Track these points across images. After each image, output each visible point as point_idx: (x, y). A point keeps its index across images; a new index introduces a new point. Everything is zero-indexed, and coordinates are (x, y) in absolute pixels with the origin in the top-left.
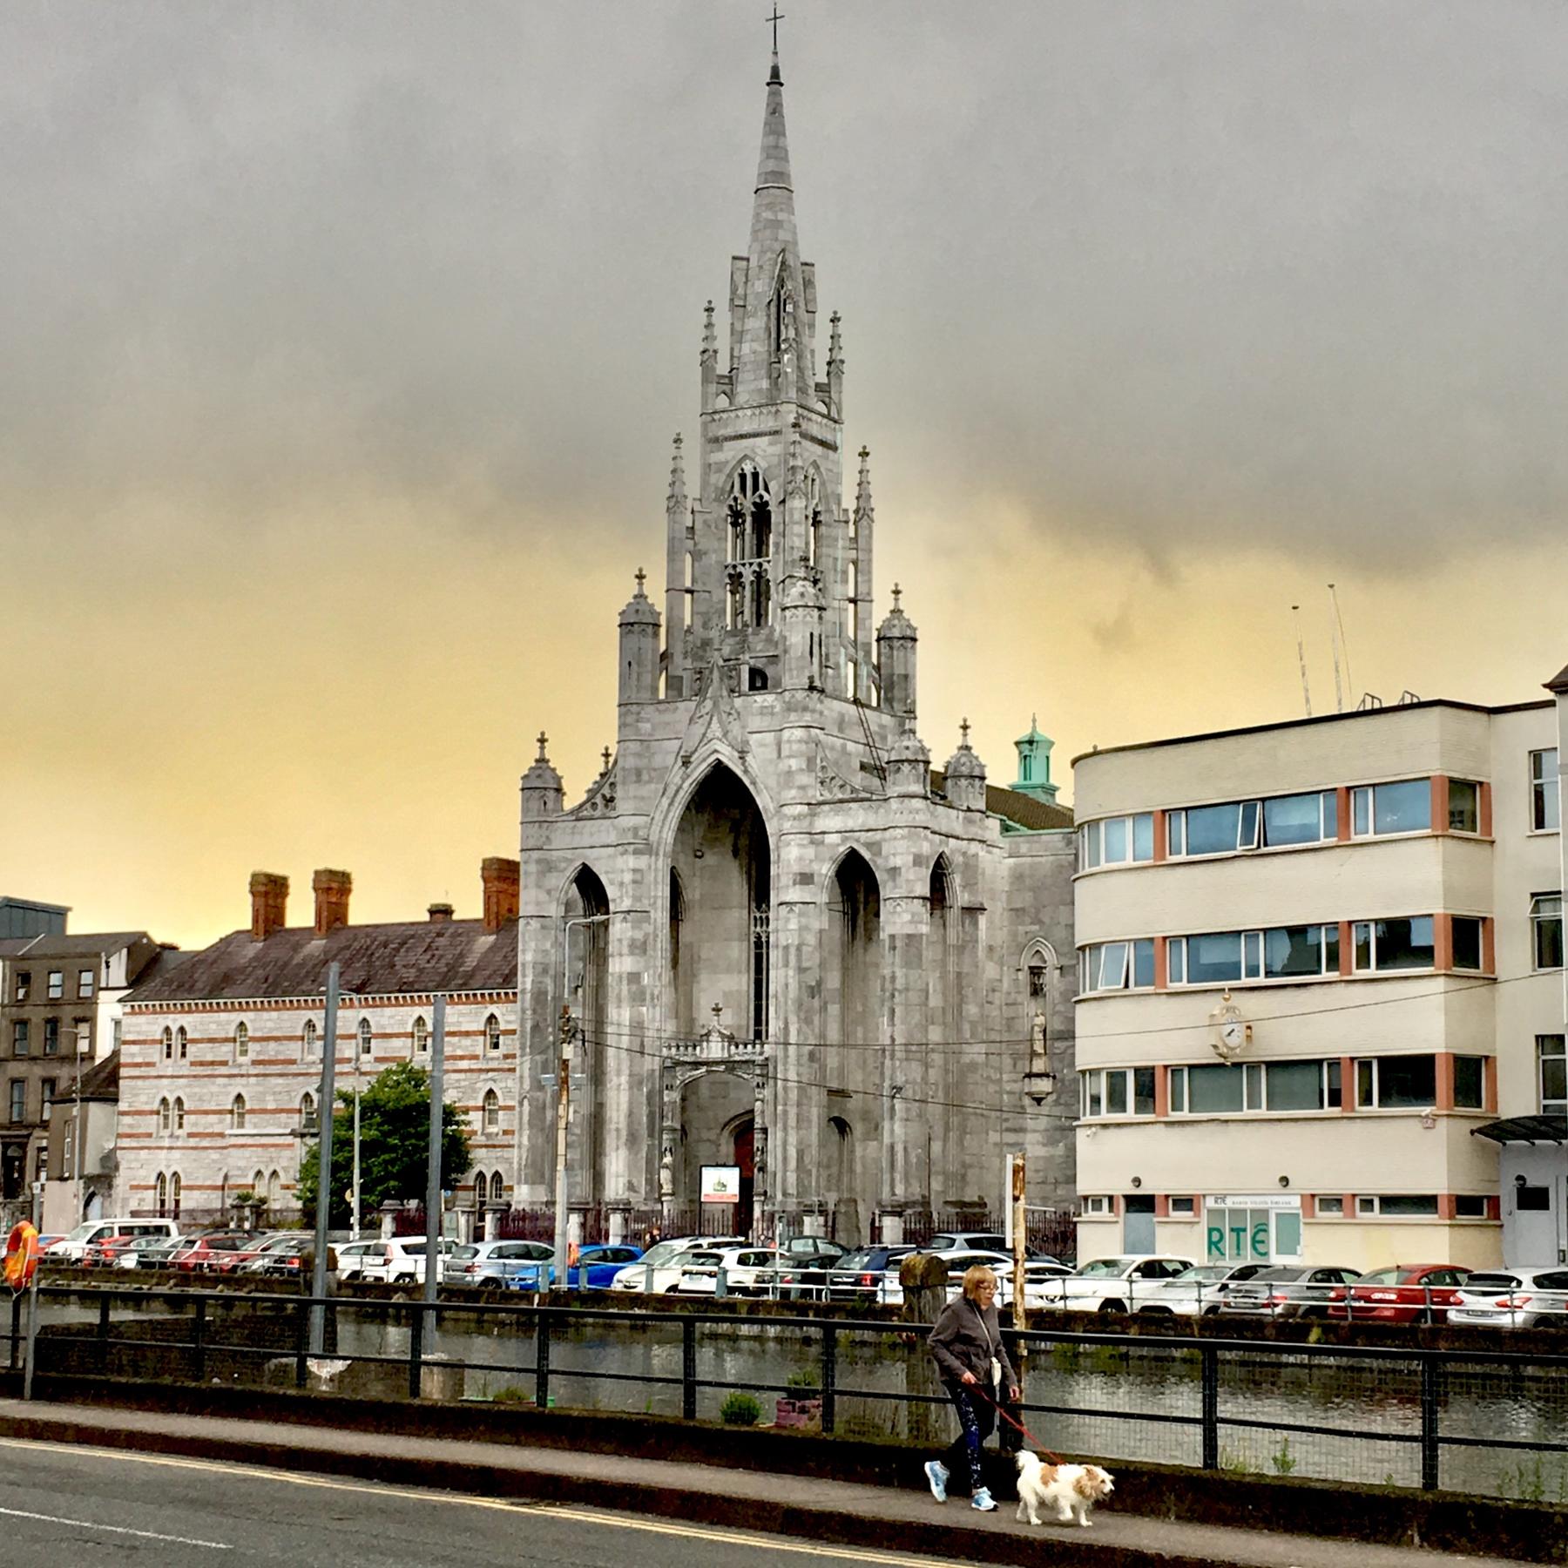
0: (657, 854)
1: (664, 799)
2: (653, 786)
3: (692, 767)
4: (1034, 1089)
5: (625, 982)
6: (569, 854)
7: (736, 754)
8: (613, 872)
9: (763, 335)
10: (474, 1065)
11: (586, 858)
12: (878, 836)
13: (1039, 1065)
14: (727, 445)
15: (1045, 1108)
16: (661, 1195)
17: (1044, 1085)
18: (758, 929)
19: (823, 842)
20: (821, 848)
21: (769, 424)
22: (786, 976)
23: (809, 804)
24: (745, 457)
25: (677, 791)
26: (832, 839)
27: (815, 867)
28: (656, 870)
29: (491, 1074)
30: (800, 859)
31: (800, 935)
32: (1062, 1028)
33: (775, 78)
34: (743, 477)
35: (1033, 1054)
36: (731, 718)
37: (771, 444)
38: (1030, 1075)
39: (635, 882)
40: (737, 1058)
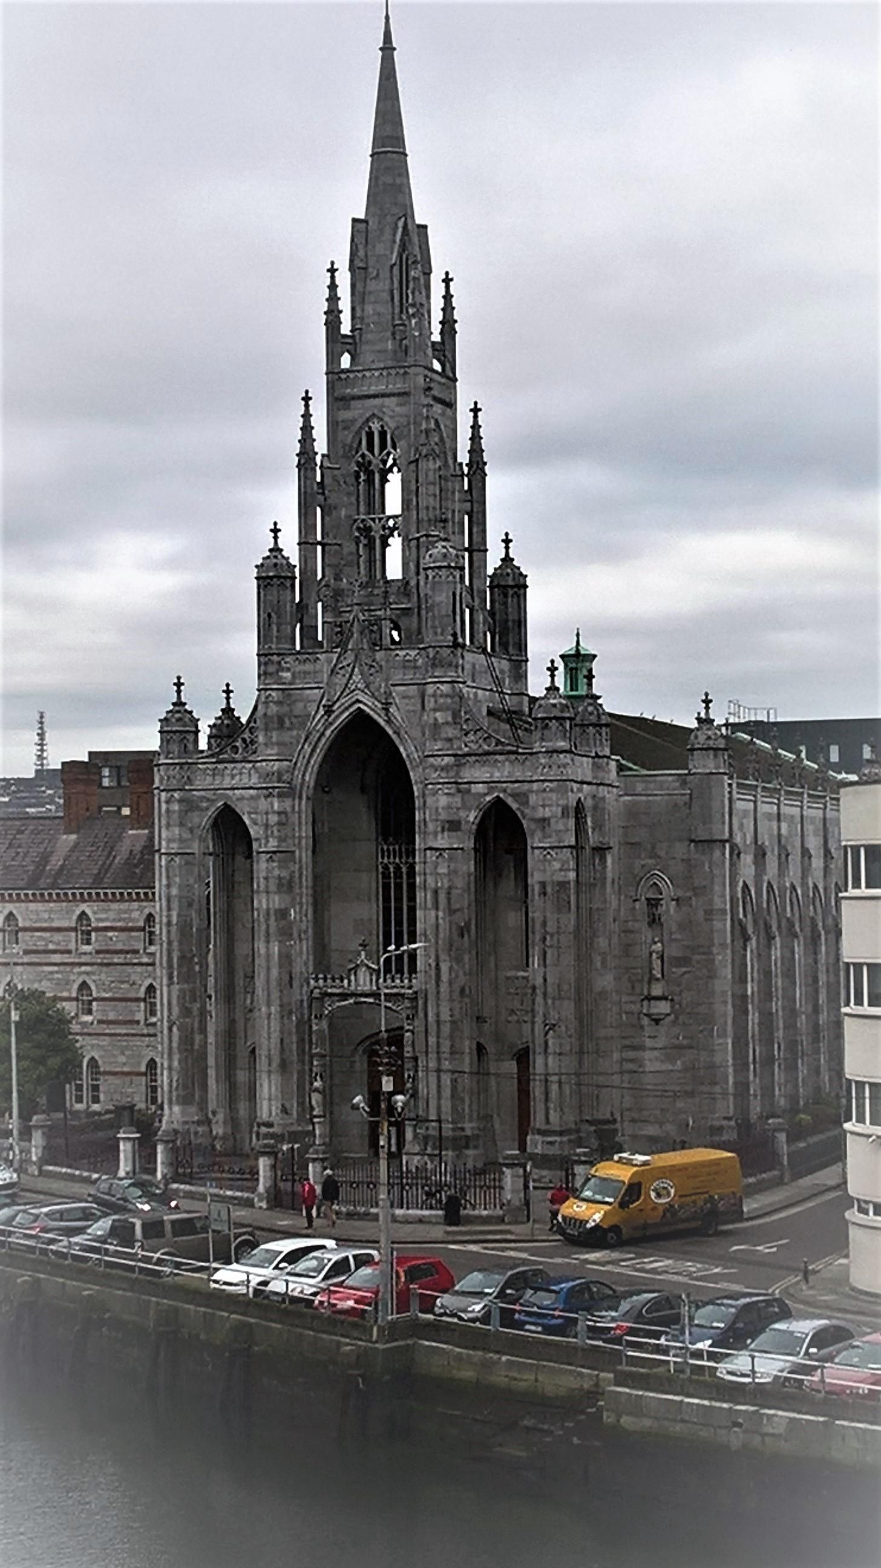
0: (300, 798)
2: (295, 733)
3: (333, 716)
4: (654, 1011)
5: (273, 918)
8: (256, 813)
9: (386, 296)
10: (66, 958)
11: (228, 797)
12: (526, 786)
13: (657, 990)
15: (662, 1029)
17: (663, 1007)
18: (386, 860)
20: (466, 797)
21: (399, 386)
22: (437, 917)
25: (319, 739)
26: (480, 788)
27: (462, 814)
28: (299, 812)
29: (83, 968)
30: (449, 807)
31: (450, 880)
32: (680, 955)
35: (652, 979)
36: (373, 670)
37: (401, 405)
38: (650, 998)
39: (280, 824)
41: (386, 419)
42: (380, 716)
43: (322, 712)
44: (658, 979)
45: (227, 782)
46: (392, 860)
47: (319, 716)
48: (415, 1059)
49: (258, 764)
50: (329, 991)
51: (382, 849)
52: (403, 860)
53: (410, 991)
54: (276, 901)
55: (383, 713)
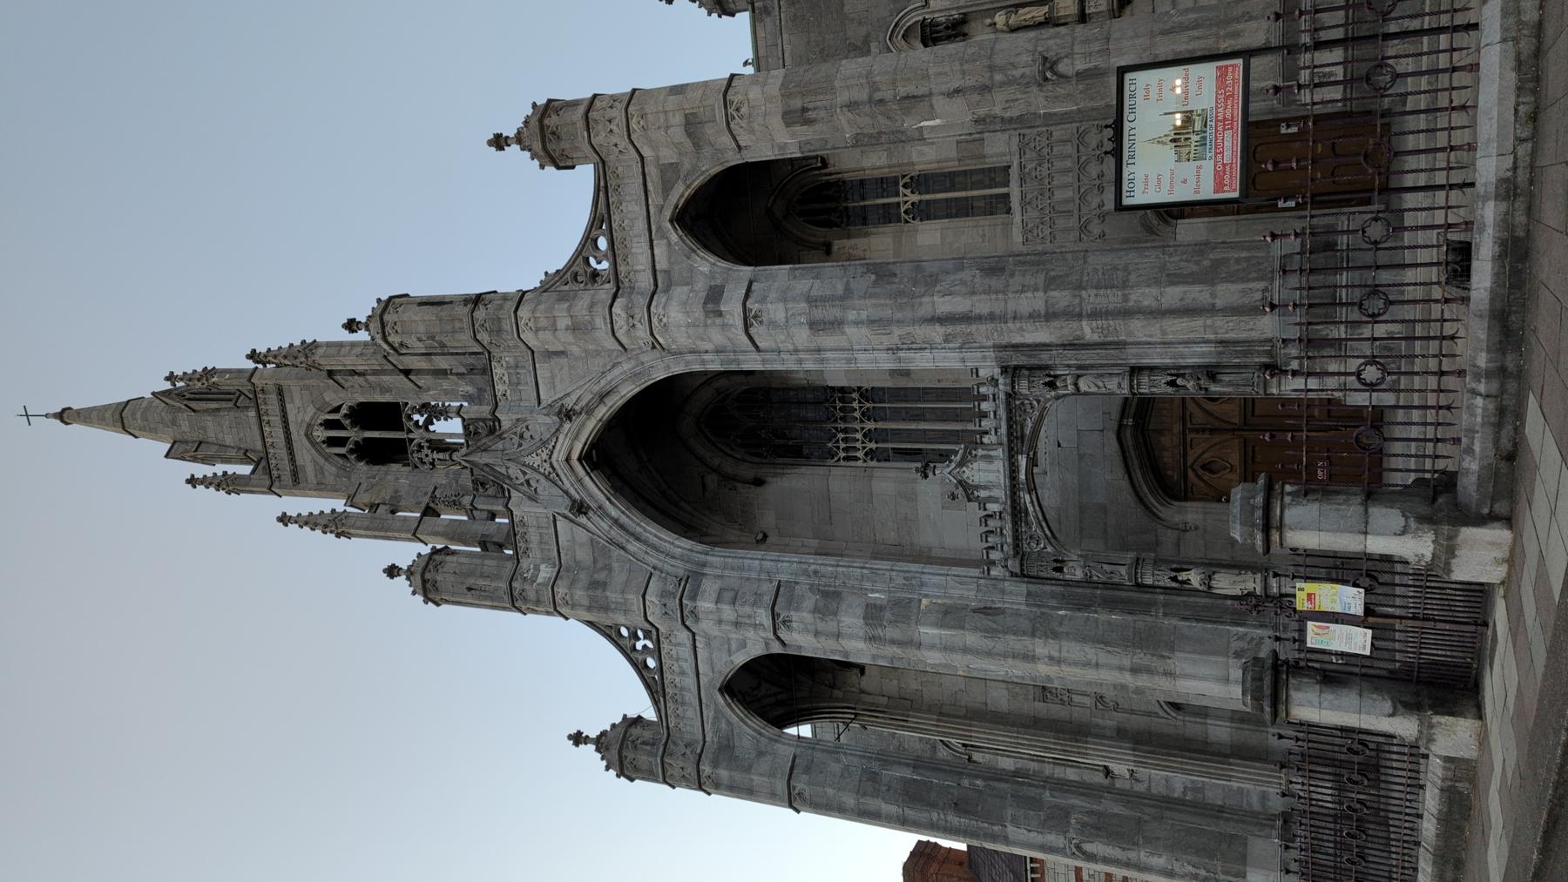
0: (704, 565)
1: (630, 547)
2: (615, 565)
5: (880, 632)
6: (709, 714)
7: (567, 426)
12: (652, 170)
14: (299, 461)
16: (1267, 596)
19: (665, 271)
23: (615, 297)
24: (308, 436)
25: (622, 527)
27: (701, 286)
31: (794, 299)
33: (64, 416)
34: (332, 442)
36: (527, 435)
40: (1003, 430)
41: (307, 419)
42: (583, 425)
43: (583, 519)
44: (1051, 10)
45: (690, 682)
46: (858, 445)
47: (589, 525)
48: (1135, 371)
50: (1009, 540)
51: (844, 459)
52: (857, 426)
53: (1001, 381)
54: (851, 619)
55: (577, 421)
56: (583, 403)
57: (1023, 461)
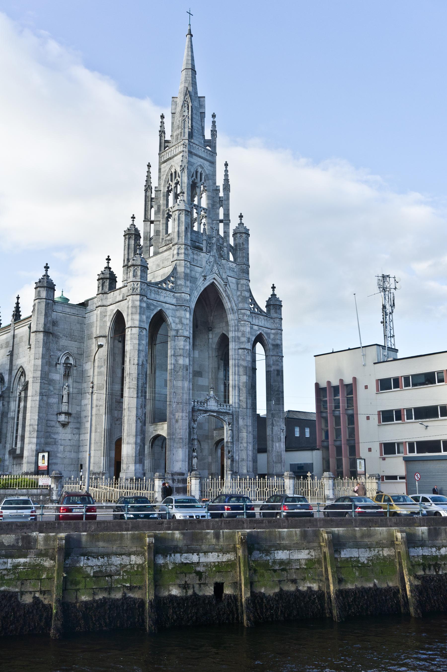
8: (175, 317)
11: (163, 307)
24: (200, 166)
34: (197, 172)
45: (162, 299)
49: (176, 295)
55: (223, 286)
56: (227, 290)
57: (215, 414)
